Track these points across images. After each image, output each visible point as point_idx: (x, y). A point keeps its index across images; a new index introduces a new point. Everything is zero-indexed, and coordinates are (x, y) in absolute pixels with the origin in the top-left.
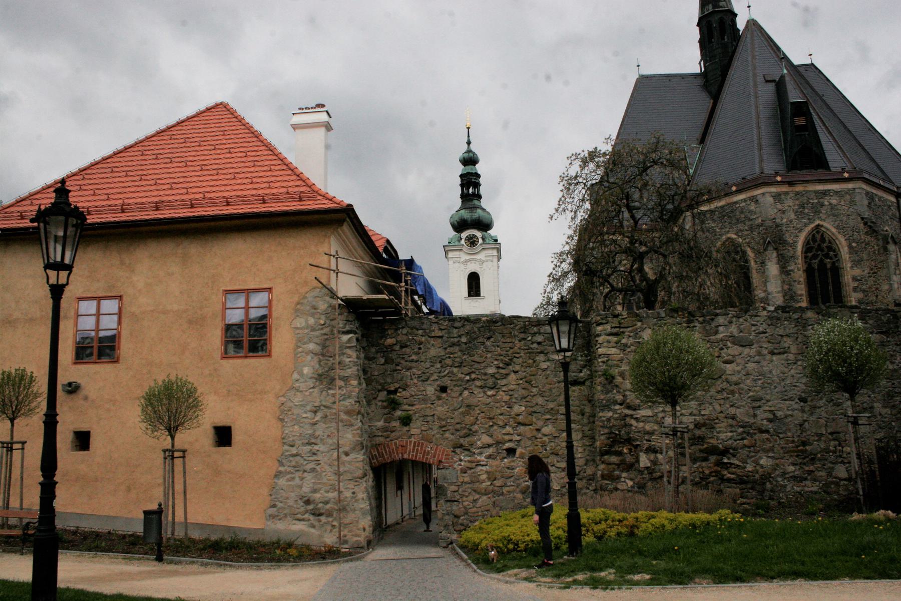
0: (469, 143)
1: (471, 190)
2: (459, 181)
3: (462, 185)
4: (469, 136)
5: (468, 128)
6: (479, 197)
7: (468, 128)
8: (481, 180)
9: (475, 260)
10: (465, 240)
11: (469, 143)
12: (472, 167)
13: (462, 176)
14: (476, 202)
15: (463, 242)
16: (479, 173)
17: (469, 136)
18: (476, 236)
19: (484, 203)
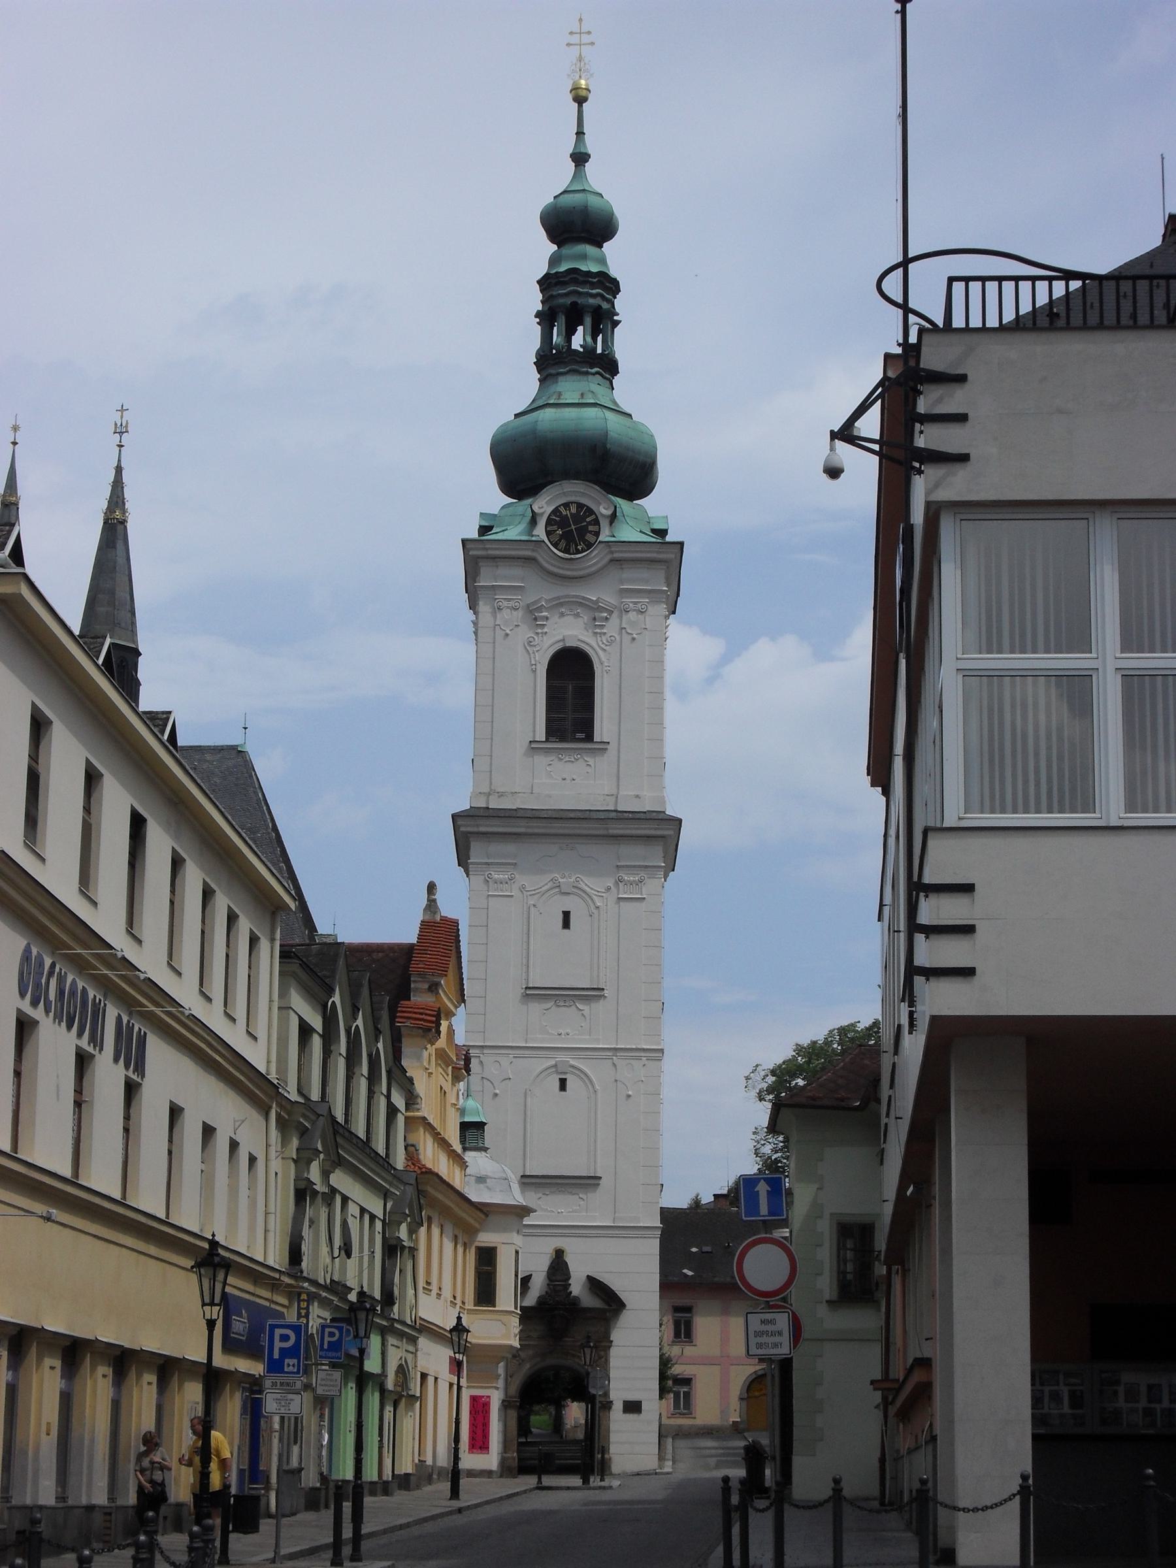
0: (580, 158)
1: (578, 341)
2: (534, 300)
3: (546, 318)
4: (580, 133)
5: (580, 100)
6: (608, 366)
7: (580, 100)
8: (620, 303)
9: (584, 604)
10: (549, 522)
11: (580, 158)
12: (590, 249)
13: (547, 283)
14: (592, 386)
15: (540, 532)
16: (613, 273)
17: (580, 133)
18: (590, 512)
19: (624, 390)
